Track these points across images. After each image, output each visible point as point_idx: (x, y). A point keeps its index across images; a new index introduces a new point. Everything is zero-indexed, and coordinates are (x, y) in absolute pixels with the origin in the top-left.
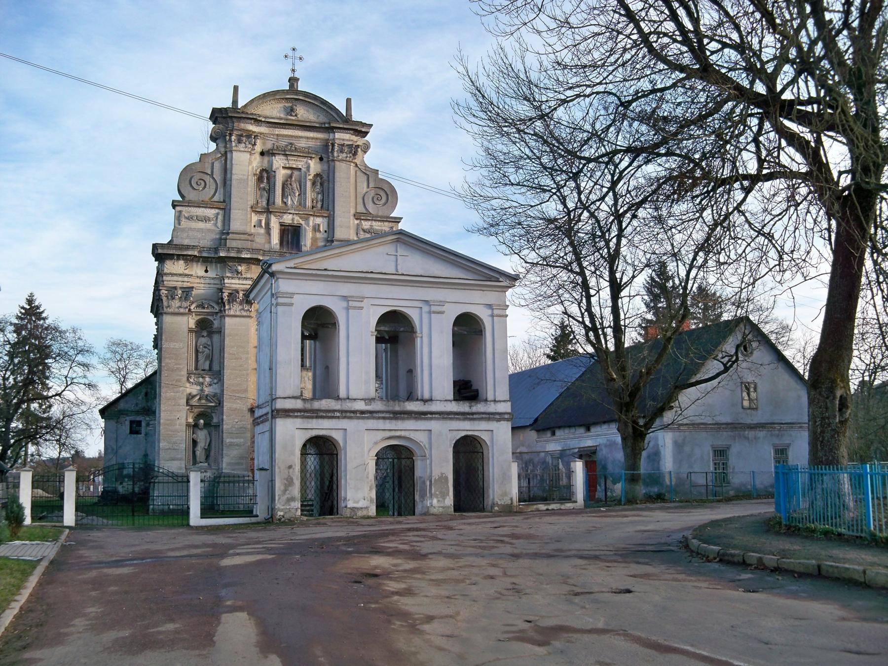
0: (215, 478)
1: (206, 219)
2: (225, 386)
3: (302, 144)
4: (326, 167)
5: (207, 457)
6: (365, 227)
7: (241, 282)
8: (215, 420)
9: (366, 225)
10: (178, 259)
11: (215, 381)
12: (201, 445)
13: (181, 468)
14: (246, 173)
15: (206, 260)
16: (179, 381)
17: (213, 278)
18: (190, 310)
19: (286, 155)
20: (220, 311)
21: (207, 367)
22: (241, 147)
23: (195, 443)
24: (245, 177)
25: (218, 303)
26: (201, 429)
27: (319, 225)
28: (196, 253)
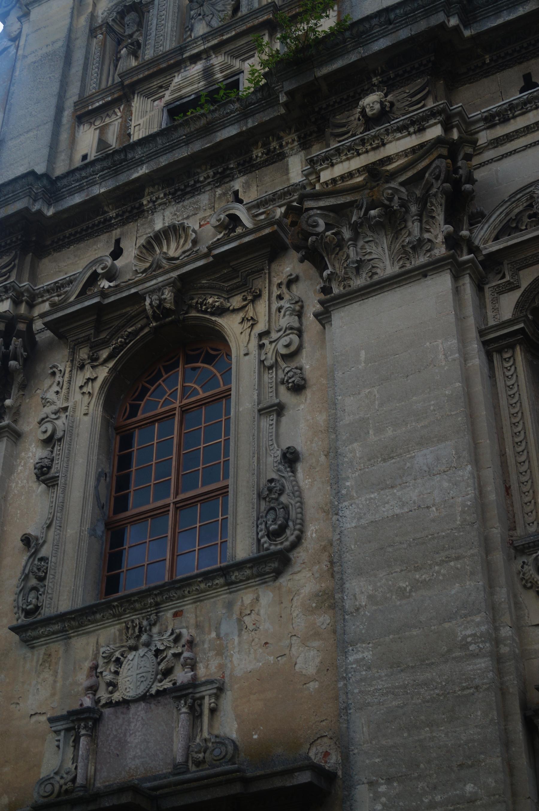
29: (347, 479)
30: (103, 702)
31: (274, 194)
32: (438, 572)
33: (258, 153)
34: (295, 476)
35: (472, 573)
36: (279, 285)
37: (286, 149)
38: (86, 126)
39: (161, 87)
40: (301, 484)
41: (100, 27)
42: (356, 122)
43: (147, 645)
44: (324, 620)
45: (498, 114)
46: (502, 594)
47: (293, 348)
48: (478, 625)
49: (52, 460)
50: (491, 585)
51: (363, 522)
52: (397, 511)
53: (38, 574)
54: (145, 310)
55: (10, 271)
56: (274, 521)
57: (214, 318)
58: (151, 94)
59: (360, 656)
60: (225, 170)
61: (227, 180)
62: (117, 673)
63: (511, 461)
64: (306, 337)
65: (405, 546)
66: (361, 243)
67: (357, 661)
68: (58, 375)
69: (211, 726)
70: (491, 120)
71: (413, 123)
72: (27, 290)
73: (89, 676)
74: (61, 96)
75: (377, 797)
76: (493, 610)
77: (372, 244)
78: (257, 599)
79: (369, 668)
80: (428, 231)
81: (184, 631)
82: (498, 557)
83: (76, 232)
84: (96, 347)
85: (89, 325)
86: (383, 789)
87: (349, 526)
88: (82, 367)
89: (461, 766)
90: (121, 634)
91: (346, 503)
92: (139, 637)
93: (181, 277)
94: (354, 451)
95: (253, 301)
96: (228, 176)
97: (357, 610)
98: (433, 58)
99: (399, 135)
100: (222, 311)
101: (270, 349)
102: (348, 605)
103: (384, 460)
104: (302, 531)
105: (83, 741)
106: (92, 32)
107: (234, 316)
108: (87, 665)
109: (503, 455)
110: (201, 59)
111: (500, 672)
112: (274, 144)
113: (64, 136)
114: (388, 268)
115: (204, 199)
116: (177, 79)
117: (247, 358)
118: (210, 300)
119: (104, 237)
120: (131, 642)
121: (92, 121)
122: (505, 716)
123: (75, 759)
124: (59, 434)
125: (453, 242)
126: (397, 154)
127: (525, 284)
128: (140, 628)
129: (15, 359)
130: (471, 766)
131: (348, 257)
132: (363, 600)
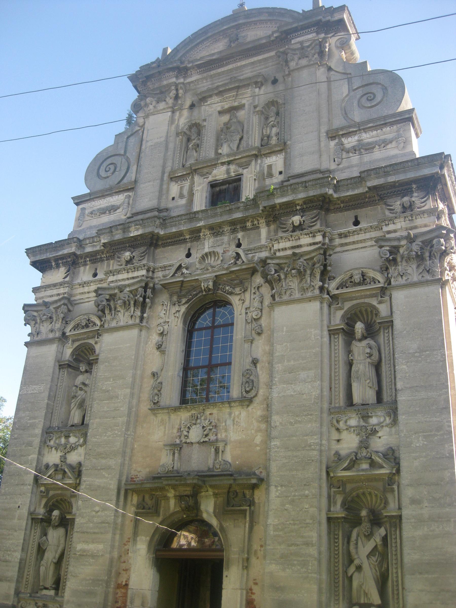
1: (113, 209)
3: (248, 73)
6: (348, 146)
7: (131, 275)
10: (58, 266)
16: (30, 444)
18: (64, 334)
23: (41, 551)
29: (275, 377)
30: (183, 441)
31: (255, 247)
32: (304, 419)
33: (249, 224)
34: (256, 369)
35: (315, 421)
36: (254, 288)
37: (260, 225)
38: (174, 183)
39: (208, 173)
40: (258, 372)
41: (181, 133)
42: (289, 225)
43: (200, 424)
44: (263, 426)
45: (344, 234)
46: (325, 429)
47: (258, 317)
48: (315, 439)
49: (163, 343)
50: (321, 425)
51: (280, 395)
52: (292, 393)
53: (158, 389)
54: (201, 288)
55: (144, 255)
56: (248, 387)
57: (228, 296)
58: (203, 175)
59: (275, 443)
60: (235, 229)
61: (235, 232)
62: (188, 432)
63: (333, 378)
64: (263, 311)
65: (294, 407)
66: (287, 281)
67: (274, 445)
68: (164, 306)
69: (222, 456)
70: (341, 236)
71: (311, 233)
72: (153, 267)
73: (178, 432)
74: (164, 167)
75: (277, 491)
76: (321, 434)
77: (291, 282)
78: (240, 413)
79: (278, 448)
80: (313, 282)
81: (213, 420)
82: (325, 415)
83: (172, 242)
85: (180, 290)
86: (279, 488)
87: (275, 395)
88: (175, 304)
89: (305, 485)
90: (190, 418)
91: (275, 387)
92: (196, 420)
93: (216, 276)
94: (279, 367)
95: (244, 292)
96: (236, 231)
97: (276, 427)
98: (321, 204)
99: (305, 236)
100: (231, 293)
101: (250, 315)
102: (273, 424)
103: (289, 373)
104: (257, 392)
106: (178, 134)
107: (236, 296)
108: (177, 427)
109: (330, 375)
110: (225, 164)
111: (321, 455)
112: (256, 222)
113: (165, 187)
114: (297, 295)
115: (226, 238)
116: (215, 172)
117: (240, 316)
118: (227, 288)
119: (183, 246)
120: (194, 422)
121: (177, 181)
122: (321, 470)
123: (173, 460)
124: (165, 333)
125: (322, 289)
126: (304, 245)
127: (346, 309)
128: (197, 417)
129: (148, 298)
130: (308, 485)
131: (282, 286)
132: (278, 424)
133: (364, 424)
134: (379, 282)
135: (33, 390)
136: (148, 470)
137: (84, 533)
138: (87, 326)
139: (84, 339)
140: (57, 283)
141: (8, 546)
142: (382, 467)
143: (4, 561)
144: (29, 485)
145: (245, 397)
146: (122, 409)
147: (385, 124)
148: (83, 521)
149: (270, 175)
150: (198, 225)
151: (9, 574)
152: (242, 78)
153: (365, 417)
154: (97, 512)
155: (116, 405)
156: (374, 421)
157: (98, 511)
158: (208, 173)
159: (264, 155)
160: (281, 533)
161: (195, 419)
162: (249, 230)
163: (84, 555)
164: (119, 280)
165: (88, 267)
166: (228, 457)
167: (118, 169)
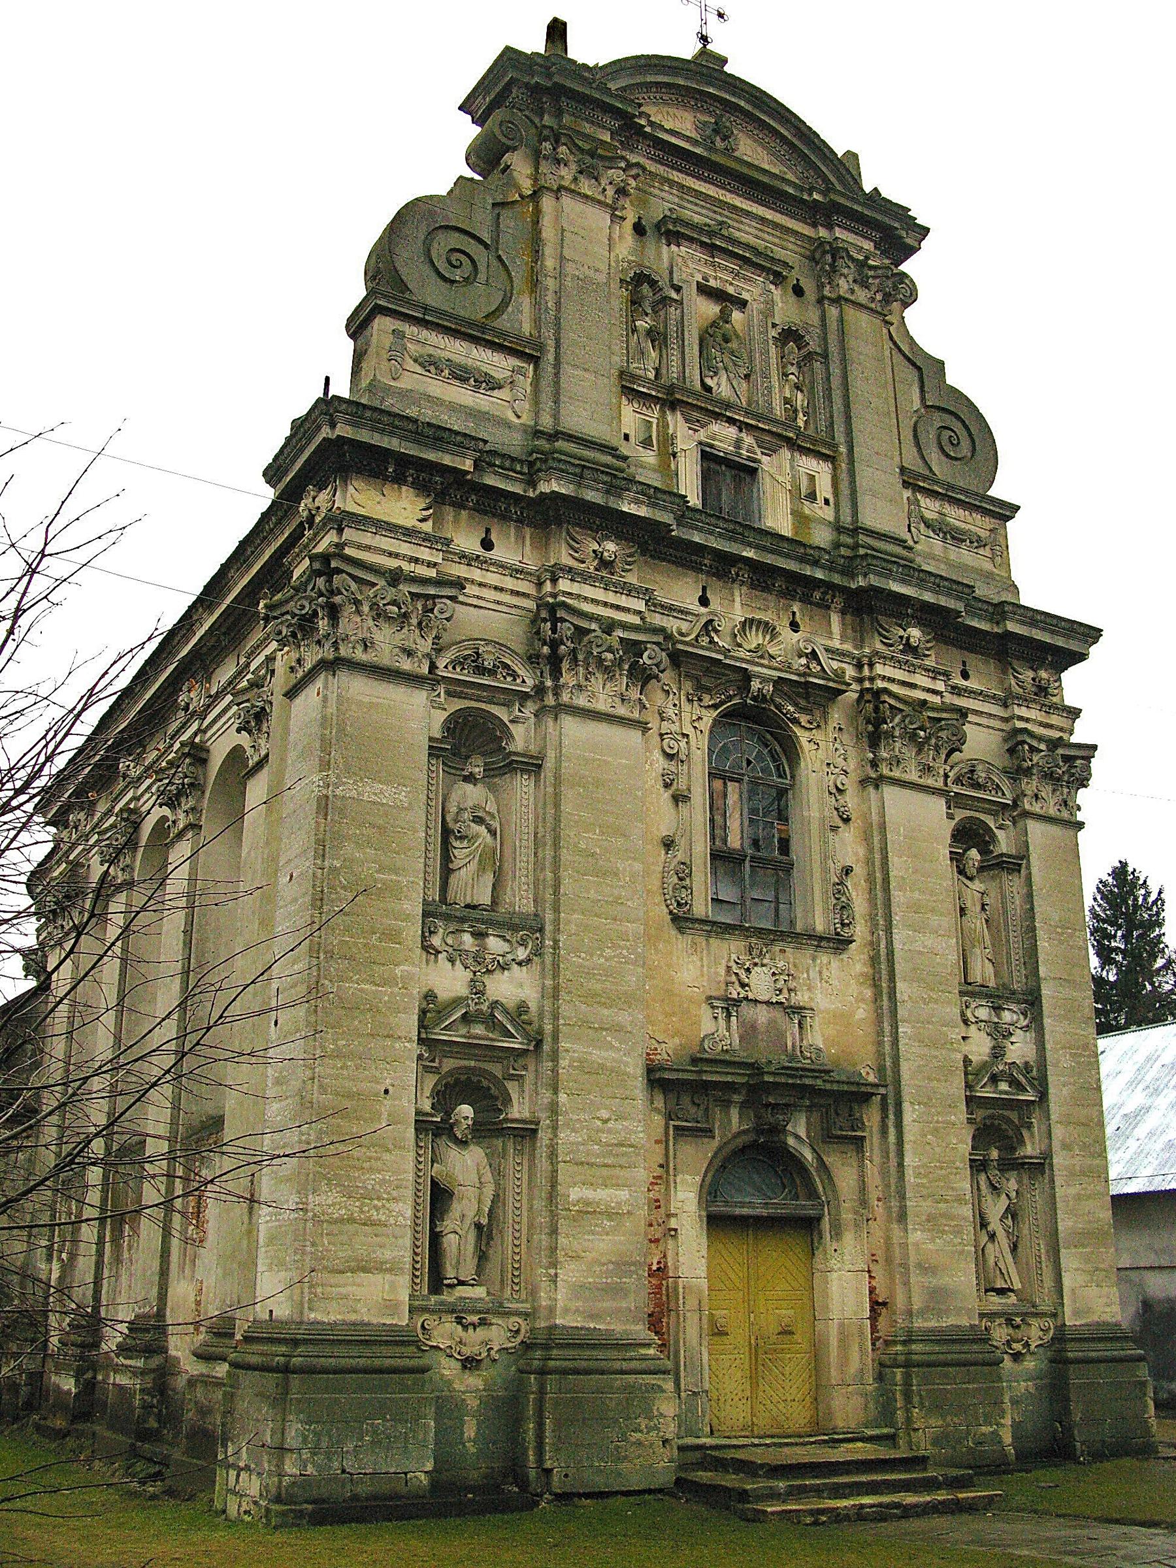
0: (527, 1346)
2: (565, 974)
3: (746, 233)
4: (813, 316)
5: (482, 1257)
6: (929, 515)
7: (611, 598)
8: (518, 1110)
9: (930, 508)
10: (399, 480)
11: (522, 953)
12: (465, 1210)
13: (391, 1306)
14: (603, 267)
15: (491, 505)
16: (392, 935)
17: (516, 572)
18: (433, 667)
19: (711, 249)
20: (540, 690)
21: (484, 897)
22: (586, 186)
23: (440, 1197)
24: (602, 278)
25: (532, 659)
26: (462, 1143)
27: (812, 478)
28: (468, 465)
33: (817, 595)
37: (833, 606)
39: (698, 421)
75: (914, 1110)
84: (700, 688)
100: (796, 721)
105: (734, 1019)
108: (724, 962)
112: (828, 597)
133: (996, 1020)
134: (1003, 794)
135: (375, 794)
136: (677, 1040)
137: (582, 1163)
138: (492, 672)
139: (478, 699)
140: (401, 527)
141: (370, 1187)
142: (1021, 1088)
143: (365, 1224)
144: (410, 1041)
145: (838, 934)
146: (629, 903)
147: (978, 509)
148: (573, 1137)
149: (812, 496)
150: (744, 554)
151: (388, 1254)
152: (737, 234)
153: (997, 1009)
154: (606, 1121)
155: (616, 892)
156: (1007, 1016)
157: (609, 1119)
158: (698, 421)
159: (799, 446)
160: (924, 1181)
161: (756, 958)
162: (811, 603)
163: (588, 1211)
164: (586, 598)
165: (464, 514)
166: (817, 1037)
167: (482, 277)
